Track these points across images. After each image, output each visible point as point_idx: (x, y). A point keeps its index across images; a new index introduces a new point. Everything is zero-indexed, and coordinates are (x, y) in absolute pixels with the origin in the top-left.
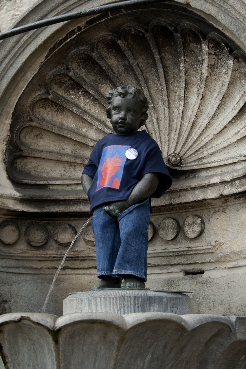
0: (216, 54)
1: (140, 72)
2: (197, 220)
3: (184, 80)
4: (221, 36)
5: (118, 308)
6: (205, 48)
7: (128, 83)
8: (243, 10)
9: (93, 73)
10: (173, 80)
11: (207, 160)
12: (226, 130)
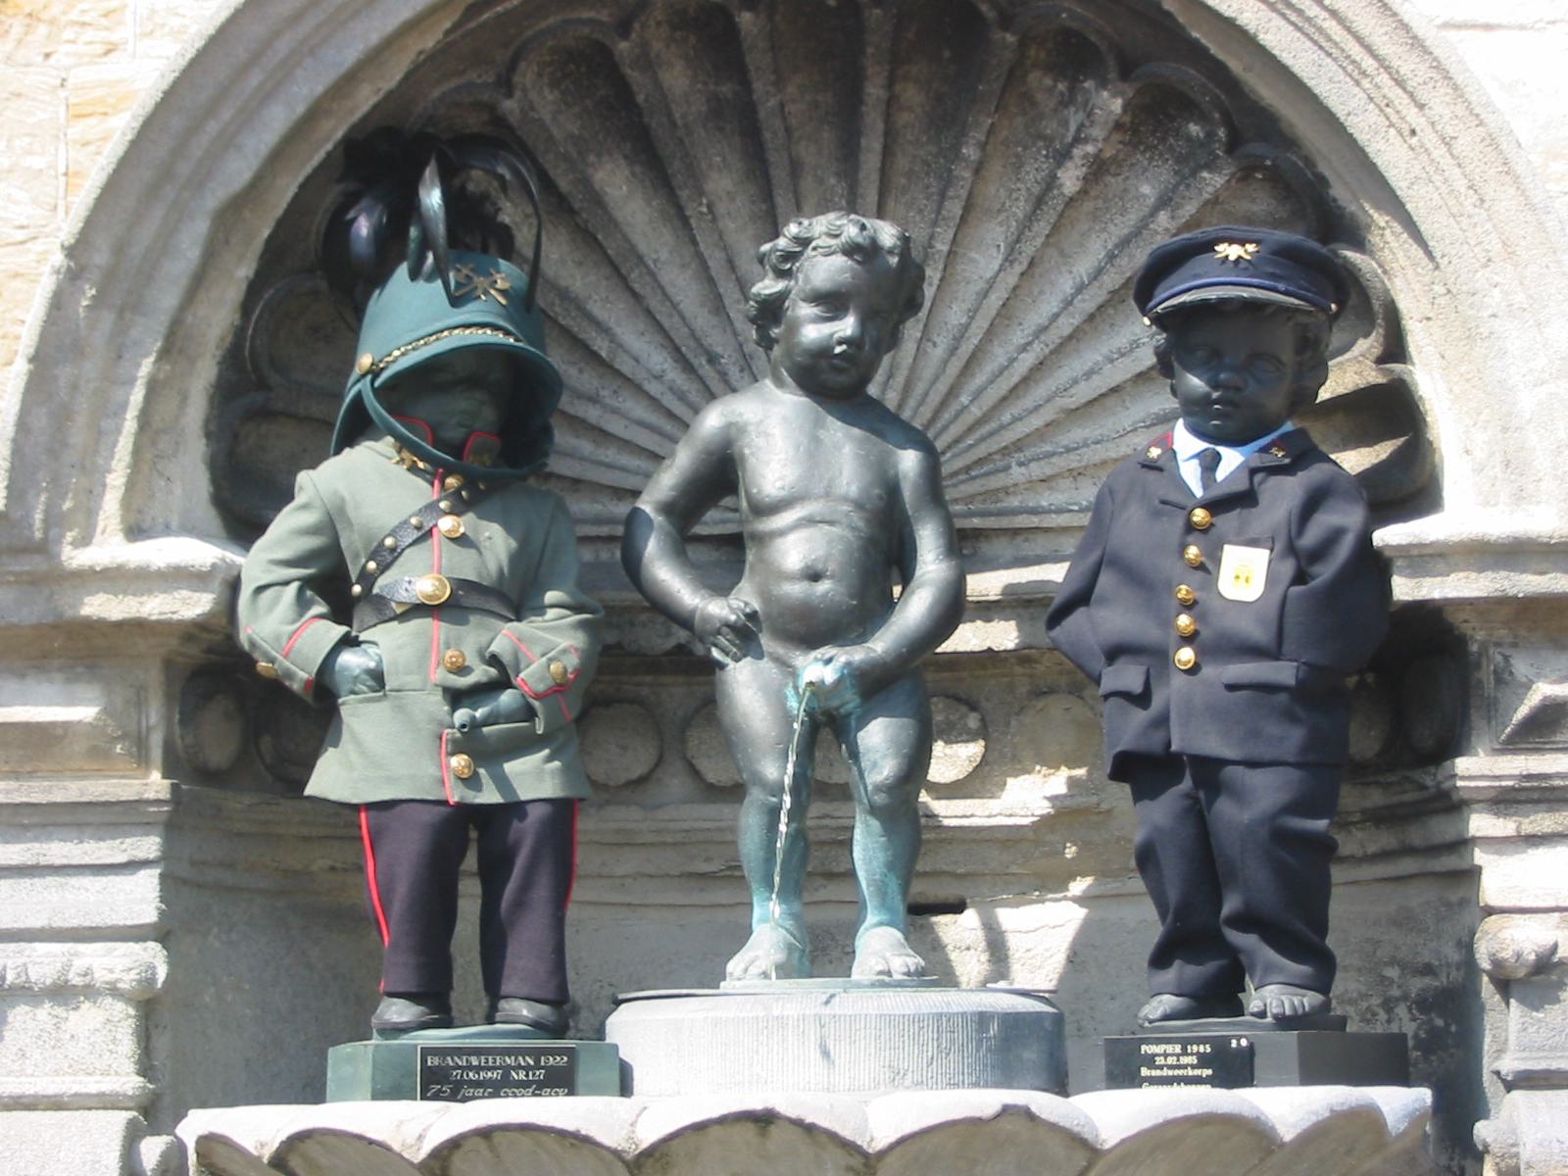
0: (1135, 131)
1: (781, 133)
2: (963, 717)
3: (964, 193)
4: (1211, 85)
5: (930, 1054)
6: (1112, 104)
7: (710, 166)
8: (1385, 38)
9: (577, 109)
10: (903, 181)
11: (1020, 497)
12: (1111, 401)
